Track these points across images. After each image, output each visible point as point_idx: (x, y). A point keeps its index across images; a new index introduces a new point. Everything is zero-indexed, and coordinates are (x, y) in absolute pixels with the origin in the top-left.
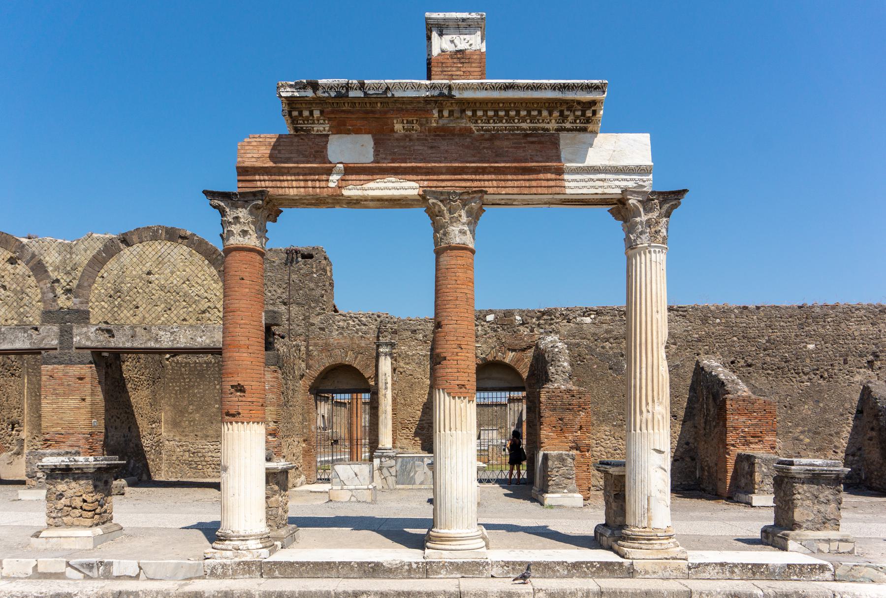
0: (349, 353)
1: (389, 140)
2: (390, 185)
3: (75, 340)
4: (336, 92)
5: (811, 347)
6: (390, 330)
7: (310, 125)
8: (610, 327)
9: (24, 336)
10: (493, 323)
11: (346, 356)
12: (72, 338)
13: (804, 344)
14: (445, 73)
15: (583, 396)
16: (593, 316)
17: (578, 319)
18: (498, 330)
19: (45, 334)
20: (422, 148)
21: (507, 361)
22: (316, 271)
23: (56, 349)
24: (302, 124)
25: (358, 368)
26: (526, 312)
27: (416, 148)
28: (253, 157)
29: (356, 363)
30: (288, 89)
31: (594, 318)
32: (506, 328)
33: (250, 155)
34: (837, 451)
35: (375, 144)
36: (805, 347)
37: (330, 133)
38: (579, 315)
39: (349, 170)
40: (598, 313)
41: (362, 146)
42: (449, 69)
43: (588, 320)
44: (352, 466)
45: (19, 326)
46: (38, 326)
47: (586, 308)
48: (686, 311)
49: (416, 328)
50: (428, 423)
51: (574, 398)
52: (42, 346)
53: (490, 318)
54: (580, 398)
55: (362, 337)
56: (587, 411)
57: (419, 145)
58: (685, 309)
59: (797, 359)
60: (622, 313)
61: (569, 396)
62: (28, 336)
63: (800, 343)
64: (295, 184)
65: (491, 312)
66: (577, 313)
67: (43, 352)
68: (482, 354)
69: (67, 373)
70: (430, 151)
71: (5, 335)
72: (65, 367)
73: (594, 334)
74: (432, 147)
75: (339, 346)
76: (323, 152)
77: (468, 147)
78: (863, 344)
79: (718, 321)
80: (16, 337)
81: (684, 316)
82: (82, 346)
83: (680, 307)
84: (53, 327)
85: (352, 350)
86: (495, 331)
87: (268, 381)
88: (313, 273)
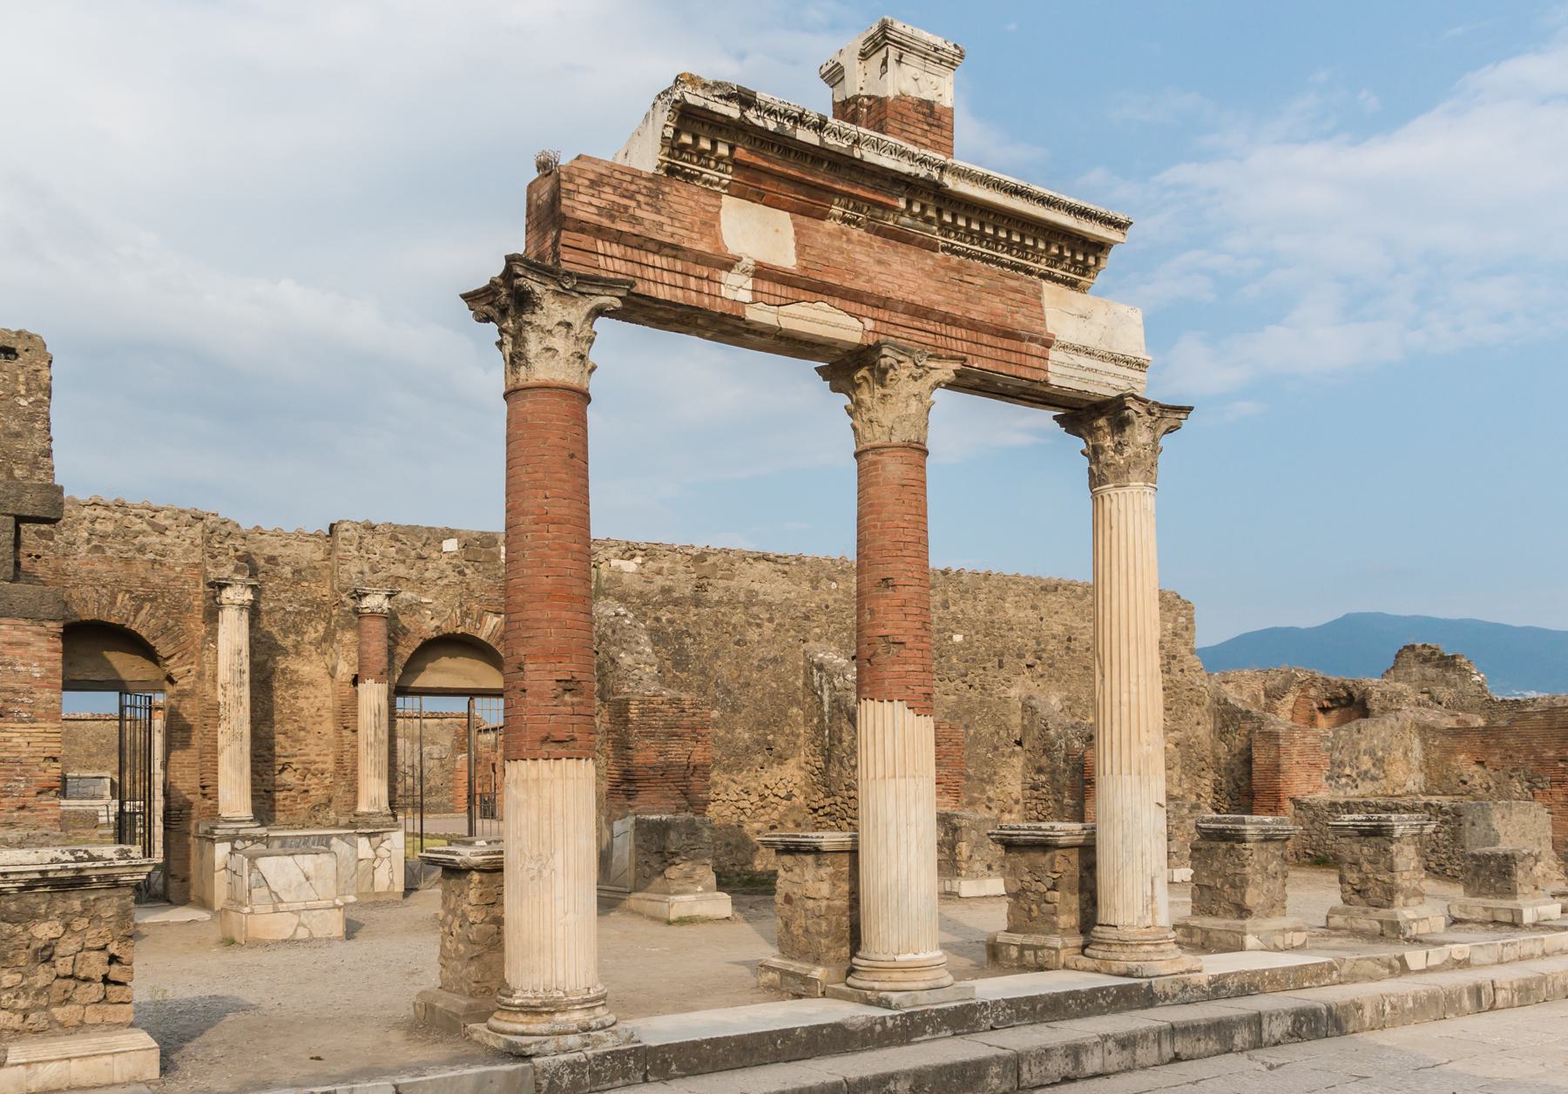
0: (120, 597)
1: (818, 231)
2: (822, 316)
4: (778, 123)
5: (958, 638)
6: (232, 552)
7: (700, 168)
8: (668, 583)
11: (113, 603)
13: (950, 633)
14: (905, 134)
15: (698, 711)
16: (639, 560)
17: (615, 562)
18: (467, 571)
20: (866, 259)
21: (483, 635)
22: (28, 390)
24: (687, 161)
25: (144, 634)
27: (857, 256)
28: (591, 204)
29: (138, 621)
30: (699, 92)
31: (642, 564)
32: (481, 568)
33: (585, 199)
34: (990, 805)
35: (796, 233)
36: (951, 637)
37: (726, 191)
38: (616, 556)
39: (762, 272)
40: (650, 552)
41: (777, 231)
42: (911, 129)
43: (630, 566)
44: (296, 857)
47: (628, 543)
48: (788, 564)
49: (276, 553)
50: (303, 763)
51: (684, 714)
53: (451, 545)
54: (694, 714)
55: (154, 562)
56: (705, 739)
57: (861, 253)
58: (787, 561)
59: (941, 657)
60: (689, 557)
61: (676, 711)
63: (945, 630)
64: (667, 277)
65: (451, 533)
66: (614, 550)
68: (432, 619)
70: (878, 268)
73: (641, 594)
74: (880, 262)
75: (94, 580)
76: (714, 226)
77: (929, 275)
78: (1022, 638)
79: (834, 585)
81: (785, 573)
83: (777, 557)
85: (127, 591)
86: (461, 573)
87: (41, 659)
88: (15, 393)
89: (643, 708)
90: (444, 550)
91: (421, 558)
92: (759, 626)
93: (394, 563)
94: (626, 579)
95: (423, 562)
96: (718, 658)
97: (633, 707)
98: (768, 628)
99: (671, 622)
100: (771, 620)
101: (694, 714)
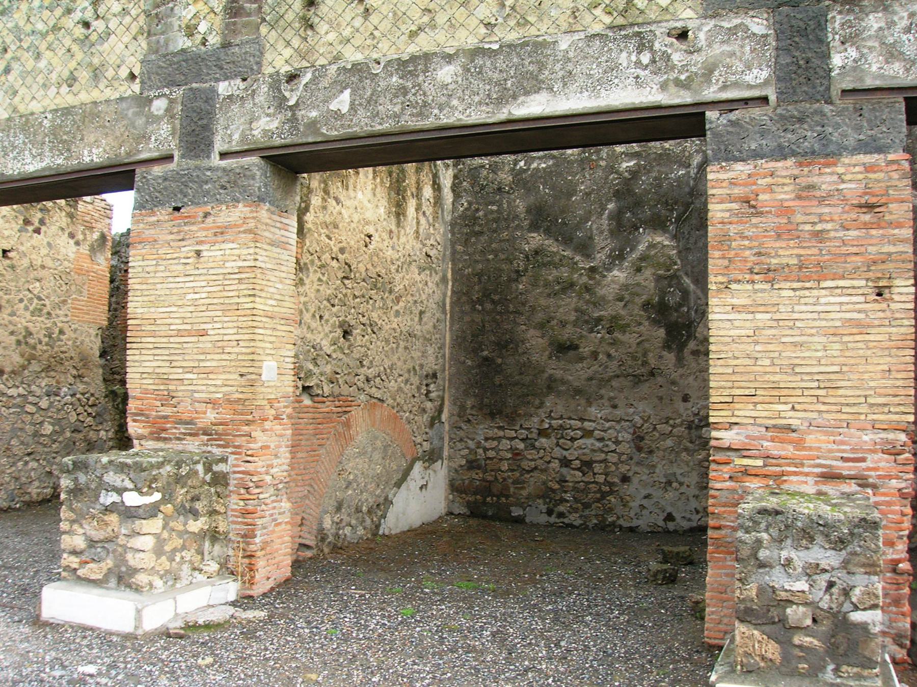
3: (837, 60)
9: (638, 63)
12: (827, 56)
19: (717, 49)
23: (765, 100)
45: (621, 27)
46: (691, 25)
52: (710, 93)
62: (653, 61)
67: (711, 115)
69: (811, 187)
71: (570, 67)
72: (801, 164)
80: (614, 67)
82: (869, 83)
84: (748, 21)
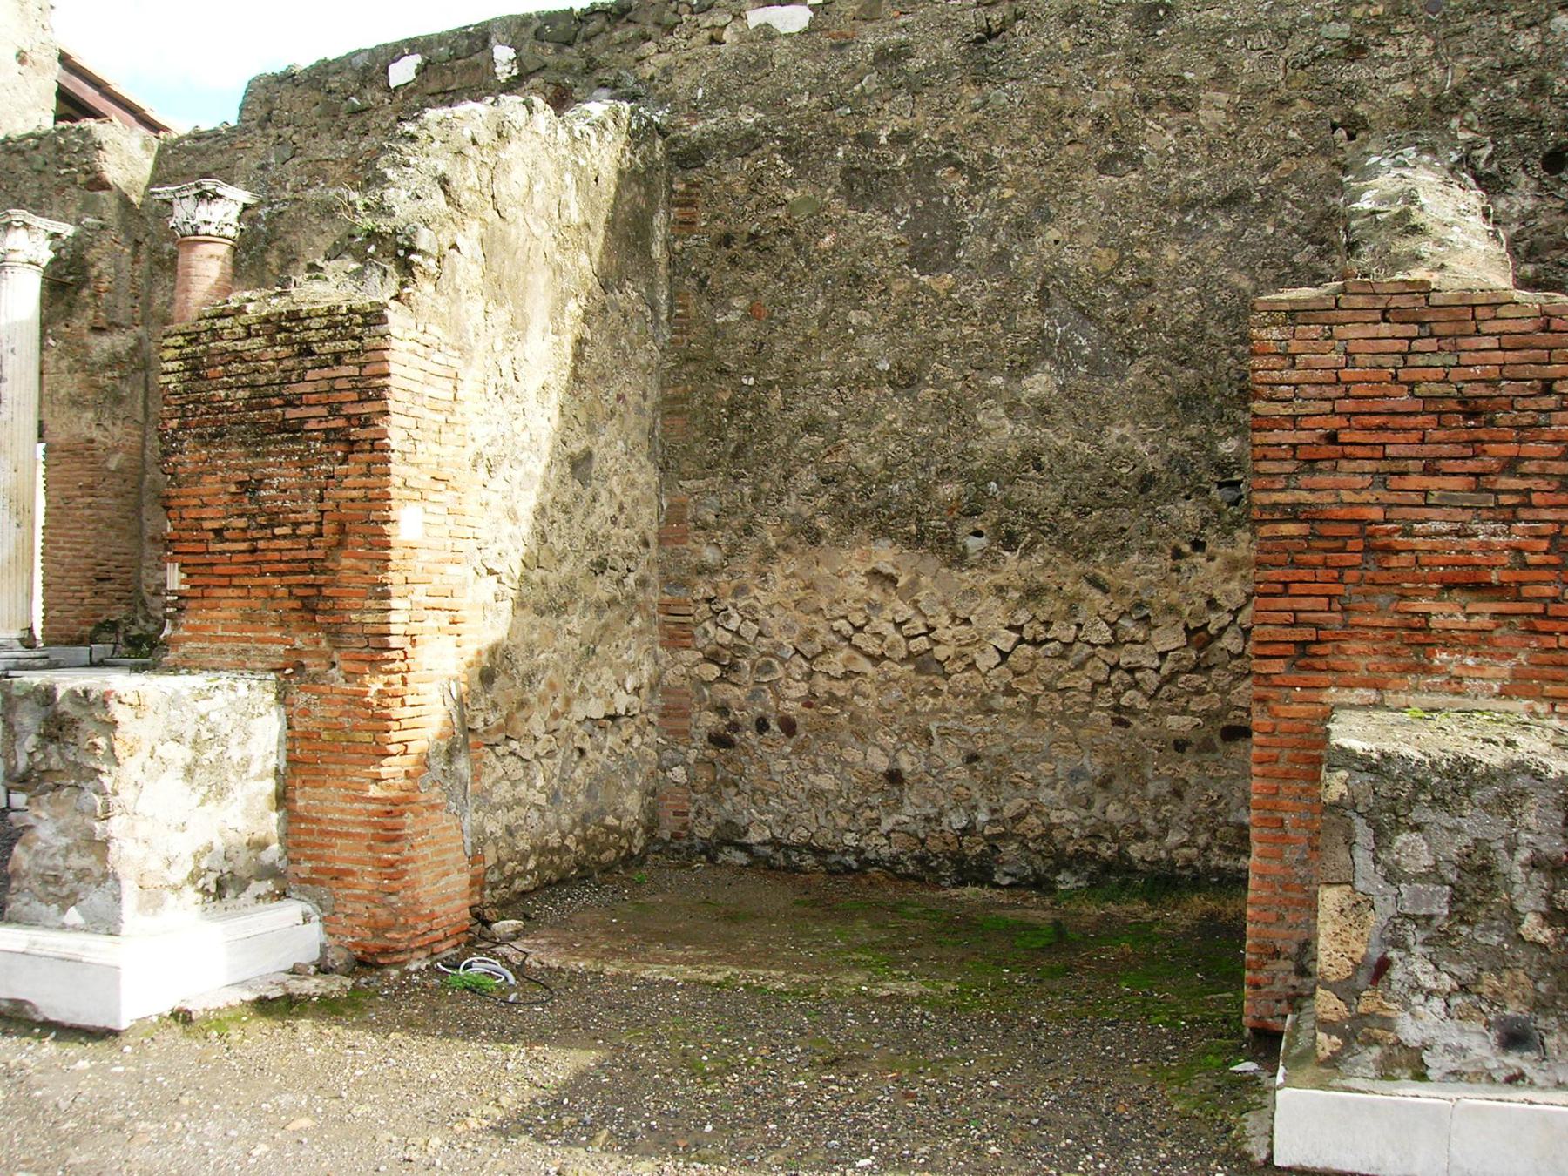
10: (413, 90)
15: (349, 345)
26: (537, 24)
54: (338, 358)
61: (285, 351)
65: (413, 45)
89: (194, 356)
90: (392, 85)
91: (356, 112)
92: (1180, 106)
93: (315, 136)
94: (781, 53)
95: (359, 120)
96: (1048, 219)
97: (169, 354)
98: (1213, 111)
99: (901, 139)
100: (1223, 78)
101: (338, 358)
